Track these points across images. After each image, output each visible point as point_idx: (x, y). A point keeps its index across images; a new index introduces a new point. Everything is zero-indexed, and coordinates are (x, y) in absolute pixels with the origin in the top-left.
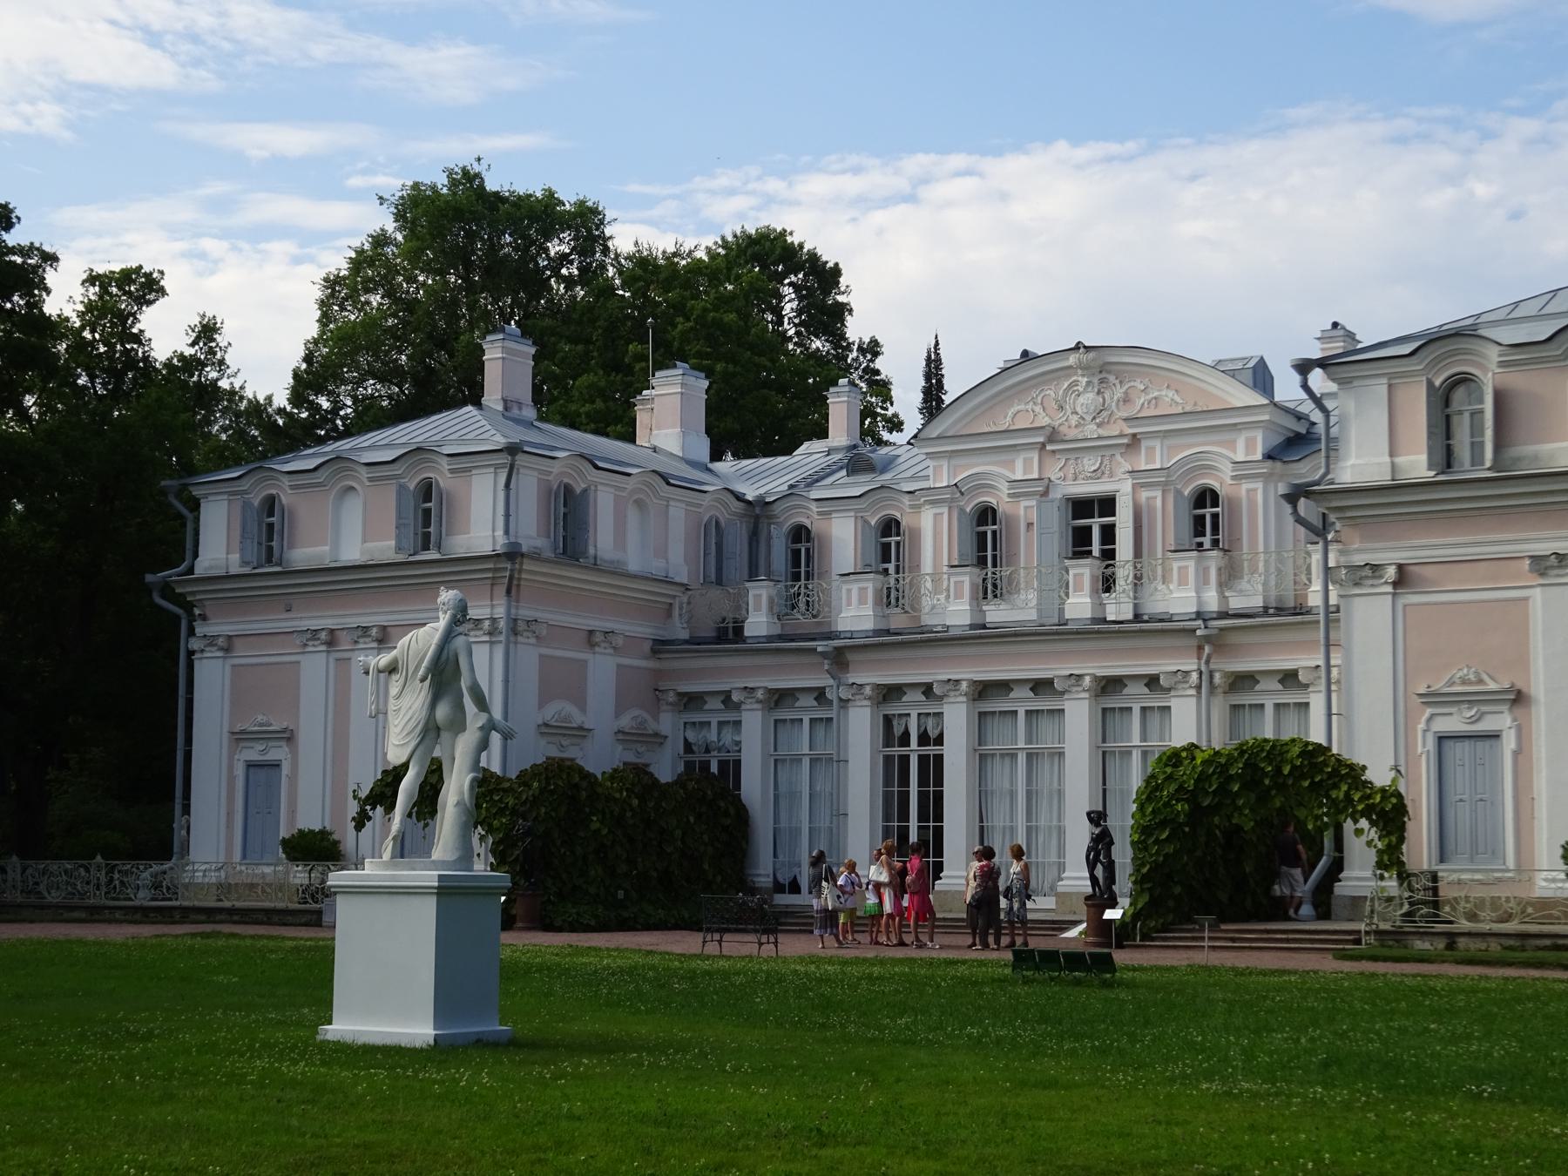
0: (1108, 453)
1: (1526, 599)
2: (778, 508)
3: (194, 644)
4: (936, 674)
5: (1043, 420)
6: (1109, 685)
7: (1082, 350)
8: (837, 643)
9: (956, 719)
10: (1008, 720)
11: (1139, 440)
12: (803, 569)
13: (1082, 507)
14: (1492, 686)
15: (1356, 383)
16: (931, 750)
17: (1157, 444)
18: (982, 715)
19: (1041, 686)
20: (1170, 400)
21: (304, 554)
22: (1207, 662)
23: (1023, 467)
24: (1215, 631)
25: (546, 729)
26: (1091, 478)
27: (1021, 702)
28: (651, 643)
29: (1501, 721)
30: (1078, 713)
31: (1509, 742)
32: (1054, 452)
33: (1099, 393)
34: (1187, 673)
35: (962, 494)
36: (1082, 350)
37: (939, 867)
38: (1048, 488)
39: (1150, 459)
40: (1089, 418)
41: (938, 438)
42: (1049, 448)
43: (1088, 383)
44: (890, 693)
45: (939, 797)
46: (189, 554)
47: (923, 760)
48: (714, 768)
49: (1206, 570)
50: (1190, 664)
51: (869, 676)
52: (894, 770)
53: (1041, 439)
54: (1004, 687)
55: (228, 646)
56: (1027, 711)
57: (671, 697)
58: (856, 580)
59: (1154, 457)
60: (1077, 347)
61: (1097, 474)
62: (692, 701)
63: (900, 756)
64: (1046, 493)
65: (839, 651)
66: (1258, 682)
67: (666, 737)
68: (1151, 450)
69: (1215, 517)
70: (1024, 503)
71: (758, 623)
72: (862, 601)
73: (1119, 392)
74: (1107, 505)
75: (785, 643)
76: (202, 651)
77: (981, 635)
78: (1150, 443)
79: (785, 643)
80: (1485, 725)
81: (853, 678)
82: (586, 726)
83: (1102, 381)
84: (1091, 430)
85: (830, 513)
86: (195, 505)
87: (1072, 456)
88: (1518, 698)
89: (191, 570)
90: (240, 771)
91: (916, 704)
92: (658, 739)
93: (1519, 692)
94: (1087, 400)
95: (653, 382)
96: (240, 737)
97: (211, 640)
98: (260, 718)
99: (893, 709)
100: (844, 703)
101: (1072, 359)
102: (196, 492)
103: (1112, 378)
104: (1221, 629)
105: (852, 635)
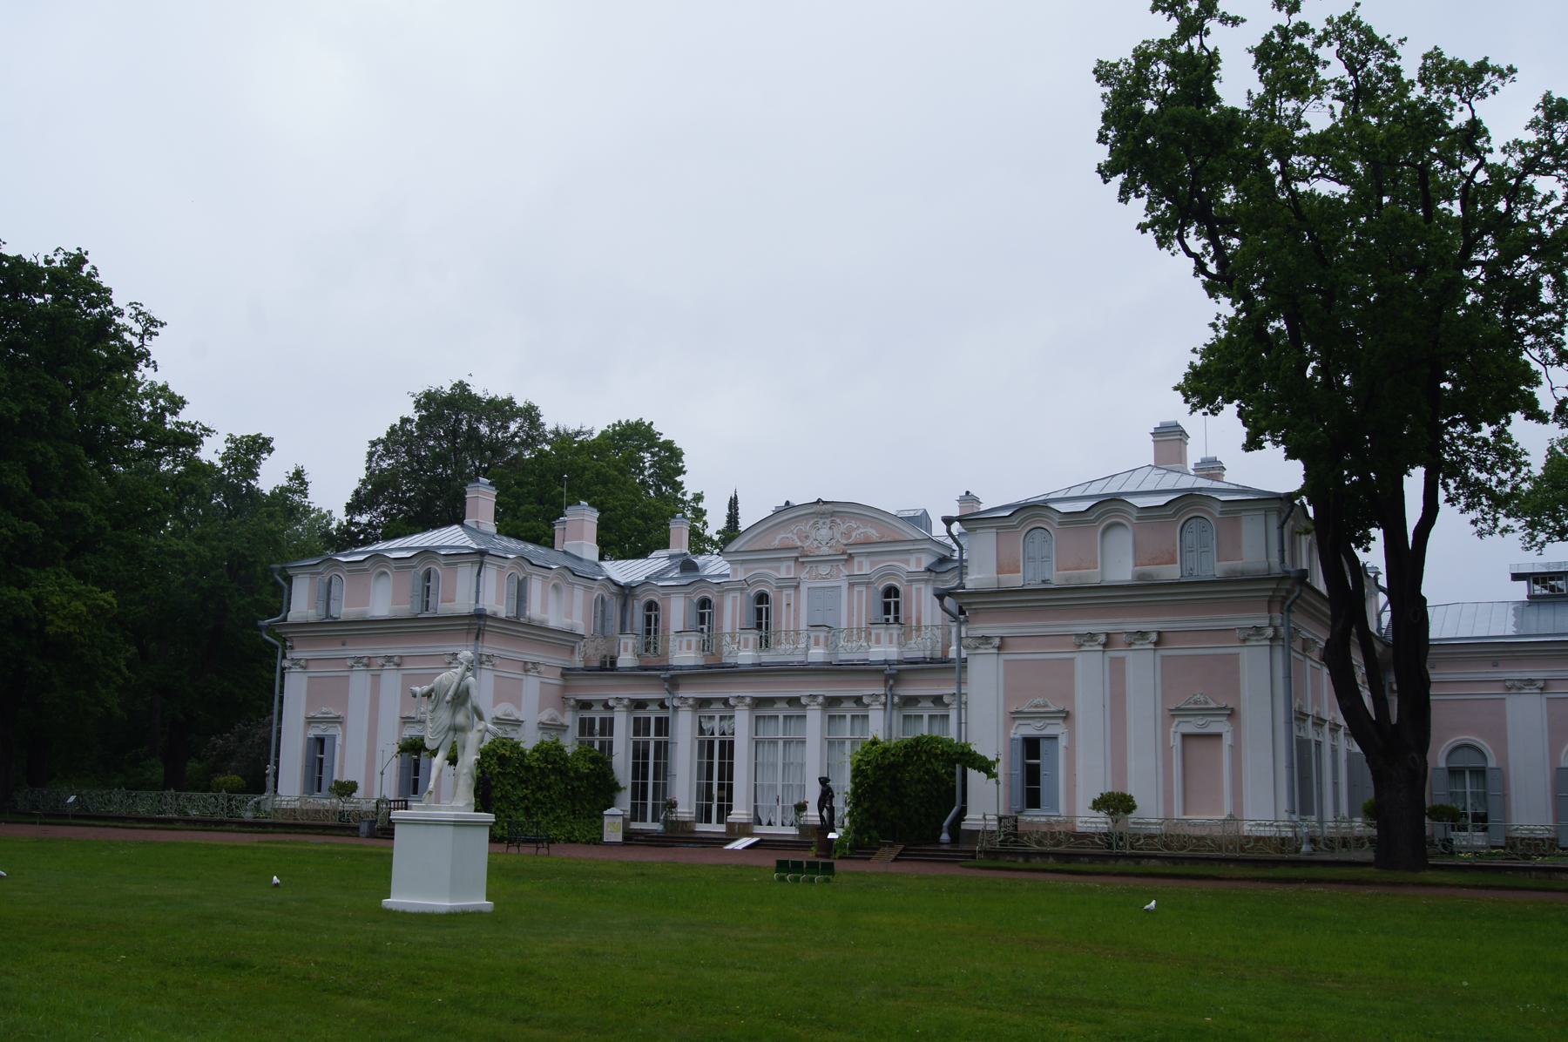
0: (834, 564)
1: (1073, 659)
2: (638, 591)
3: (286, 663)
4: (730, 692)
5: (799, 544)
6: (832, 702)
7: (821, 503)
8: (672, 672)
9: (742, 723)
10: (773, 722)
11: (853, 557)
12: (652, 627)
14: (1053, 709)
15: (978, 531)
16: (727, 738)
17: (863, 559)
18: (758, 718)
19: (793, 701)
20: (874, 534)
22: (891, 690)
23: (785, 571)
24: (894, 672)
25: (498, 721)
26: (824, 578)
27: (781, 710)
28: (561, 670)
30: (815, 718)
31: (1062, 742)
32: (803, 562)
33: (830, 528)
34: (878, 696)
35: (748, 585)
36: (821, 503)
37: (730, 808)
38: (799, 583)
39: (860, 569)
40: (824, 543)
41: (736, 552)
42: (800, 560)
43: (824, 523)
44: (703, 703)
45: (731, 765)
46: (285, 610)
47: (722, 743)
48: (597, 747)
49: (891, 635)
50: (880, 690)
51: (690, 692)
52: (706, 748)
53: (796, 555)
54: (770, 701)
55: (304, 666)
56: (784, 716)
57: (572, 702)
58: (687, 635)
59: (864, 567)
60: (819, 501)
61: (829, 576)
62: (585, 705)
63: (708, 741)
64: (797, 587)
65: (672, 677)
66: (919, 702)
67: (568, 726)
68: (860, 563)
69: (897, 604)
70: (785, 592)
71: (626, 659)
72: (689, 647)
73: (843, 528)
75: (642, 672)
76: (290, 668)
77: (759, 671)
79: (642, 672)
81: (683, 693)
82: (521, 719)
84: (825, 550)
85: (669, 594)
86: (289, 580)
88: (1066, 716)
89: (285, 619)
91: (718, 711)
92: (563, 728)
93: (1068, 713)
94: (824, 532)
95: (566, 512)
96: (311, 721)
97: (296, 662)
98: (324, 710)
99: (706, 712)
100: (676, 708)
102: (290, 572)
103: (838, 521)
104: (899, 671)
105: (681, 668)
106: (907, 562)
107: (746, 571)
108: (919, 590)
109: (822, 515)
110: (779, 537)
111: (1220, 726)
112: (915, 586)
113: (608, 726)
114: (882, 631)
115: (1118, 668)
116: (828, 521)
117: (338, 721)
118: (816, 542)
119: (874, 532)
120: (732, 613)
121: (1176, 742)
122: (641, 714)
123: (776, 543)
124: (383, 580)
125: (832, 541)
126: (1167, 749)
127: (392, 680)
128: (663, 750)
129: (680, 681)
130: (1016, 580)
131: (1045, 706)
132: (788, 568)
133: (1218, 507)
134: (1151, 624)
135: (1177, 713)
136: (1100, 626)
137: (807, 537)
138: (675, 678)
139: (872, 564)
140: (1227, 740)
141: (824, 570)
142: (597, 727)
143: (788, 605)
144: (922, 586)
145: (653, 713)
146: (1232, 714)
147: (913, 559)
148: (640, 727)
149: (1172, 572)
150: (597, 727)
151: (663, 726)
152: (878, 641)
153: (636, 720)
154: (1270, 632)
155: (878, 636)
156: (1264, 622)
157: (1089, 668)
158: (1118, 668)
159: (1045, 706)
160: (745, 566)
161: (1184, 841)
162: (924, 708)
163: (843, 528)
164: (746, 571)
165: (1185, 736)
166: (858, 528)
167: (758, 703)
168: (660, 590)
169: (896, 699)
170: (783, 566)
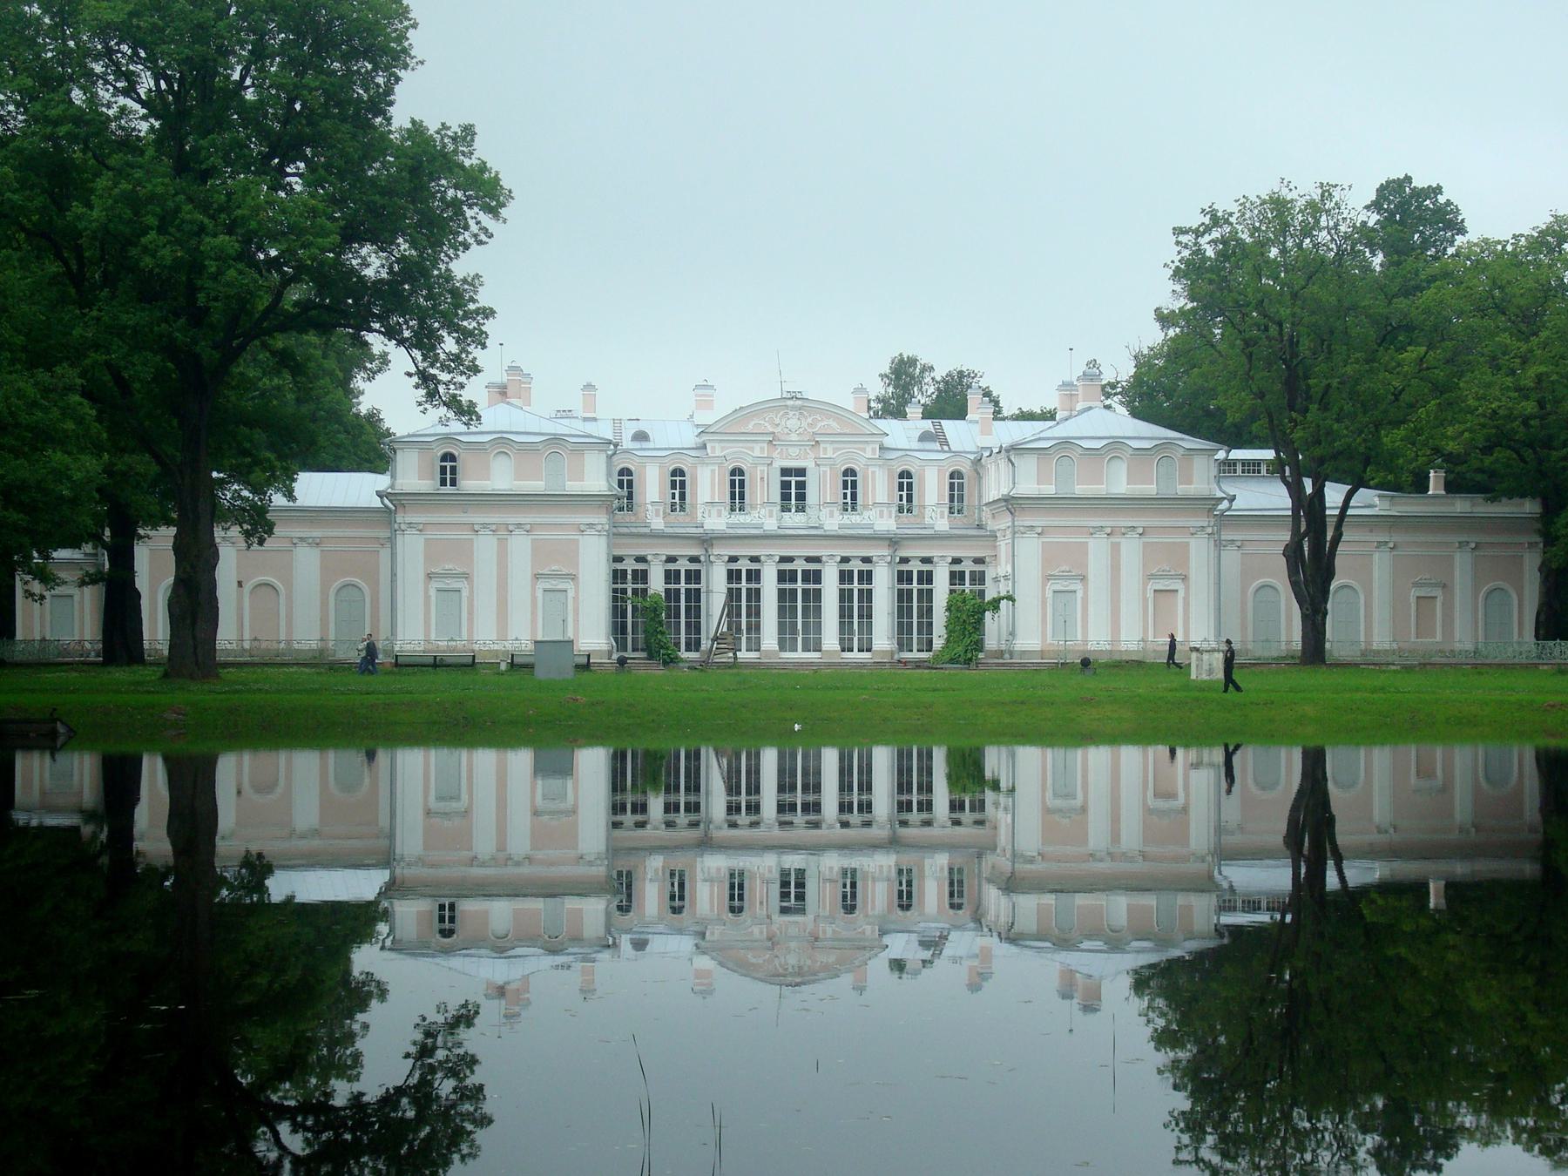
5: (771, 430)
13: (785, 472)
17: (828, 445)
20: (835, 426)
21: (468, 484)
23: (758, 450)
29: (1077, 586)
31: (1080, 594)
44: (733, 559)
49: (890, 512)
54: (790, 559)
61: (798, 457)
68: (825, 449)
74: (801, 472)
78: (824, 445)
80: (1072, 588)
83: (801, 414)
84: (794, 437)
87: (784, 448)
90: (433, 593)
94: (793, 423)
96: (429, 576)
98: (450, 567)
101: (790, 403)
106: (864, 450)
107: (723, 449)
108: (873, 472)
109: (793, 408)
110: (753, 423)
111: (1177, 585)
112: (871, 469)
113: (642, 576)
114: (885, 509)
115: (1116, 549)
116: (797, 413)
117: (466, 576)
118: (786, 430)
119: (835, 425)
120: (707, 486)
121: (1150, 595)
122: (672, 566)
123: (750, 427)
124: (502, 460)
125: (801, 430)
126: (1145, 600)
127: (520, 546)
128: (694, 596)
129: (714, 542)
130: (1049, 490)
131: (1070, 572)
132: (762, 449)
133: (1181, 451)
134: (1140, 522)
135: (1152, 577)
136: (1108, 522)
137: (778, 425)
138: (707, 540)
139: (835, 450)
140: (1181, 594)
141: (793, 451)
142: (629, 577)
143: (762, 478)
144: (877, 469)
145: (683, 566)
146: (1185, 578)
147: (869, 448)
148: (671, 576)
149: (1150, 489)
150: (629, 577)
151: (694, 576)
152: (882, 517)
153: (668, 574)
154: (1209, 530)
155: (881, 512)
156: (1205, 524)
157: (1097, 549)
158: (1116, 549)
159: (1070, 572)
160: (723, 444)
161: (1117, 657)
162: (912, 566)
163: (810, 420)
164: (723, 449)
165: (1155, 591)
166: (822, 420)
167: (783, 559)
168: (638, 459)
169: (898, 560)
170: (757, 447)
